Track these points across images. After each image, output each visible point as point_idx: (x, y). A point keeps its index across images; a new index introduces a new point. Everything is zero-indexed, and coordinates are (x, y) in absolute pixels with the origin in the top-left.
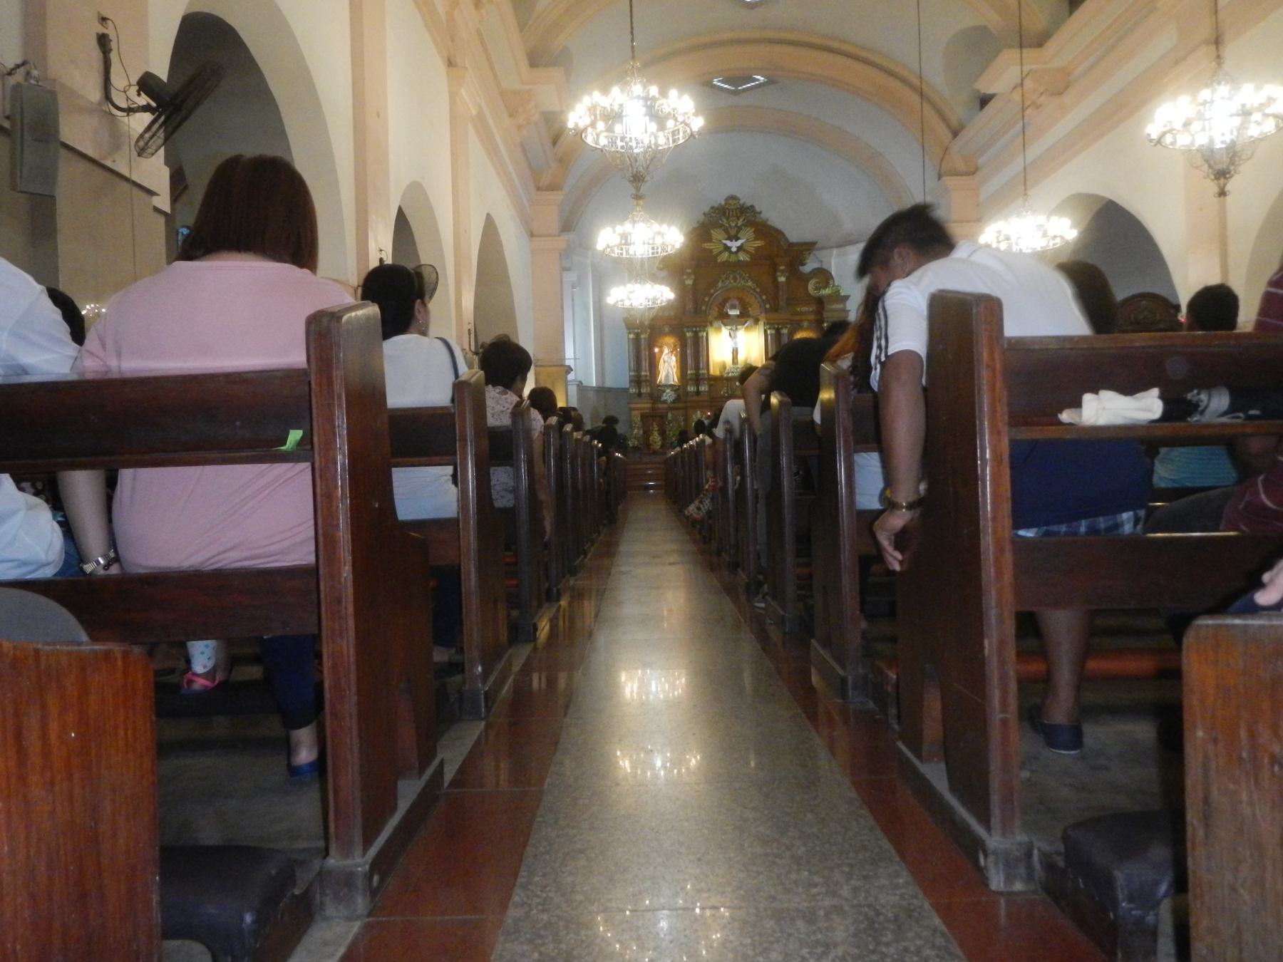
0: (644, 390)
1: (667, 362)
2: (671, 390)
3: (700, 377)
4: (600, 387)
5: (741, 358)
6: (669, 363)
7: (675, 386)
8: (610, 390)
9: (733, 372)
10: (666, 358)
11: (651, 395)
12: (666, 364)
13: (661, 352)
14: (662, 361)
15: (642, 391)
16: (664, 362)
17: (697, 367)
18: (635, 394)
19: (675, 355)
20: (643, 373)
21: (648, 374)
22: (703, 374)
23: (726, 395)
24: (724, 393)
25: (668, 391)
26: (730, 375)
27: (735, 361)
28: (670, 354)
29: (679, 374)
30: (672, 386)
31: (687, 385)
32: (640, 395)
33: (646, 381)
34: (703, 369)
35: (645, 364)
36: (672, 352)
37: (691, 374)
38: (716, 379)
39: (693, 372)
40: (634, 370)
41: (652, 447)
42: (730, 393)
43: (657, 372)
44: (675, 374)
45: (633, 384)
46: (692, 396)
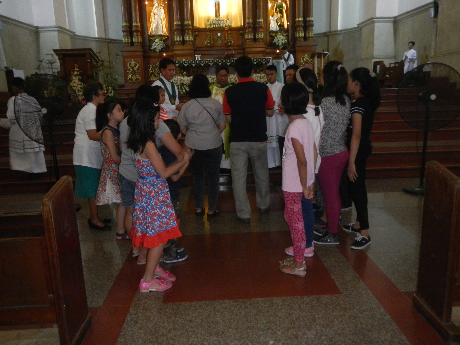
0: (135, 40)
1: (157, 14)
2: (161, 40)
3: (186, 28)
4: (101, 38)
5: (223, 13)
6: (158, 16)
7: (164, 36)
8: (112, 41)
9: (215, 24)
10: (156, 11)
11: (143, 44)
12: (156, 16)
13: (153, 6)
14: (152, 14)
15: (134, 41)
16: (155, 14)
17: (182, 19)
18: (128, 43)
19: (163, 9)
20: (134, 24)
21: (139, 25)
22: (188, 25)
23: (209, 45)
24: (207, 43)
25: (157, 40)
26: (212, 26)
27: (218, 14)
28: (160, 7)
29: (167, 27)
30: (161, 36)
31: (174, 35)
32: (132, 44)
33: (137, 31)
34: (187, 20)
35: (136, 15)
36: (161, 6)
37: (177, 25)
38: (200, 30)
39: (180, 23)
40: (126, 21)
41: (72, 97)
42: (212, 43)
43: (148, 25)
44: (164, 26)
45: (125, 34)
46: (179, 44)
